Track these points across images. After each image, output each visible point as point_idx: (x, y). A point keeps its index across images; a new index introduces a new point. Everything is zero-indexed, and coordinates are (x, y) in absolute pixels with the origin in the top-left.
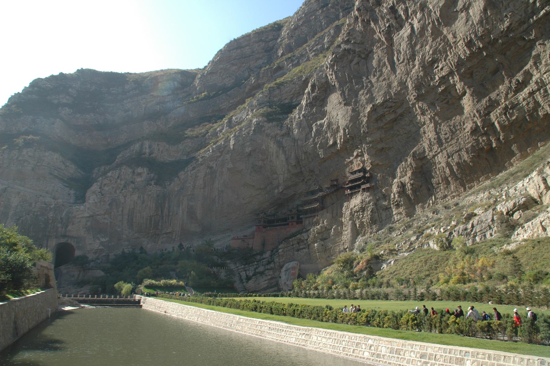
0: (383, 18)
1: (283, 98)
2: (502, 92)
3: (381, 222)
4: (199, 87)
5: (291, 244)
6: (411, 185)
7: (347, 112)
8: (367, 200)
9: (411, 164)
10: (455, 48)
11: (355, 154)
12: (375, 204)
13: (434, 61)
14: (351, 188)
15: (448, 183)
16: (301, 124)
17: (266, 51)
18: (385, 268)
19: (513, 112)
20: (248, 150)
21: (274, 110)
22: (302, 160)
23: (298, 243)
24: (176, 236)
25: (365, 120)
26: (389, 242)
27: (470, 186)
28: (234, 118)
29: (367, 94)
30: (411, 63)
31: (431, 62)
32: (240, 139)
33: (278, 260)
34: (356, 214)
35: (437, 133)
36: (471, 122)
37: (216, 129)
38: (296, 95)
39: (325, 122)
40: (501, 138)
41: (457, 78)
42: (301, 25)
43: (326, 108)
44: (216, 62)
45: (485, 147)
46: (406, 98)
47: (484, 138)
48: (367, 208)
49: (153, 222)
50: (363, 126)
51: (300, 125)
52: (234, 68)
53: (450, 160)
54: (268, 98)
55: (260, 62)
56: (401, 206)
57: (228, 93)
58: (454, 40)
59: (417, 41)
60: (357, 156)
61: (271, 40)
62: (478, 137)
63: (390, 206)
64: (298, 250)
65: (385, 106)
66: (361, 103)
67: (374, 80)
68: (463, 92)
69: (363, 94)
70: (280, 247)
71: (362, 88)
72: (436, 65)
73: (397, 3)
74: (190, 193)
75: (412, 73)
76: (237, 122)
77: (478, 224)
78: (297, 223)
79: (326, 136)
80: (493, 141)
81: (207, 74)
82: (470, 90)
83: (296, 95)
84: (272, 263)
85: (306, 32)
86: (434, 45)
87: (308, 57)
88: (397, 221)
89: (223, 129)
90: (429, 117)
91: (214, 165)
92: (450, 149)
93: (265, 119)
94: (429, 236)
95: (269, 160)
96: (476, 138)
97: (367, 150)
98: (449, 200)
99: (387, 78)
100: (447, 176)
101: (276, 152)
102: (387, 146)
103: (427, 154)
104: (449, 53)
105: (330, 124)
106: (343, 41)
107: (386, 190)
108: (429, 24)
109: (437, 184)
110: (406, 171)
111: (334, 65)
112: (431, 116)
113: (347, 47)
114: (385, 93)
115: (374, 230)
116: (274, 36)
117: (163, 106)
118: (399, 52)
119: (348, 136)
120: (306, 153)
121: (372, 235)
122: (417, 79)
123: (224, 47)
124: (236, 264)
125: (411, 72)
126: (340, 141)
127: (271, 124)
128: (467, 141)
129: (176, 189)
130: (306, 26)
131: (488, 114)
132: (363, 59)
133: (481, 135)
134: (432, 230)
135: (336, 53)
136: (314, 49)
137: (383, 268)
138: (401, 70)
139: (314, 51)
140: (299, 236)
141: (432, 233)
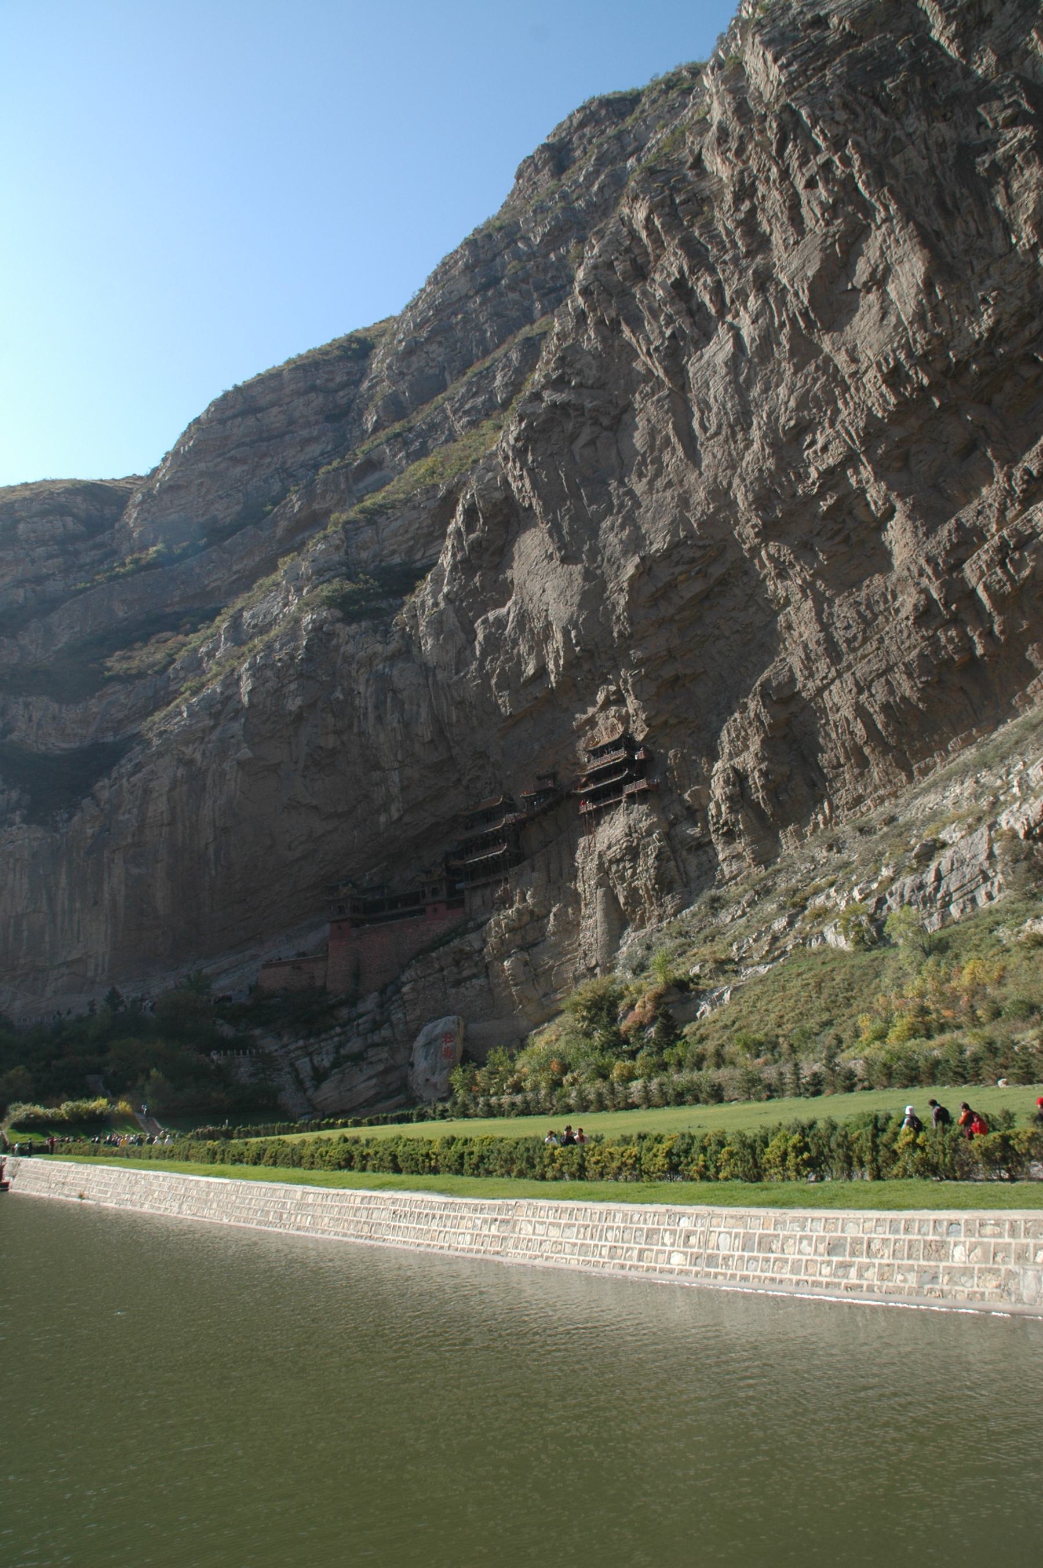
0: (655, 314)
1: (385, 552)
2: (990, 506)
4: (138, 530)
5: (437, 966)
6: (764, 774)
7: (571, 582)
8: (644, 825)
9: (757, 716)
10: (857, 389)
11: (600, 697)
12: (667, 836)
13: (804, 428)
14: (594, 796)
15: (863, 763)
16: (440, 622)
17: (330, 418)
18: (707, 1014)
19: (1022, 558)
20: (294, 704)
21: (361, 586)
23: (457, 963)
24: (96, 969)
25: (623, 600)
26: (712, 940)
27: (923, 766)
28: (246, 615)
29: (622, 527)
30: (740, 436)
31: (794, 431)
33: (400, 1015)
34: (614, 868)
35: (825, 627)
36: (913, 590)
37: (196, 650)
39: (508, 613)
40: (996, 629)
41: (866, 472)
42: (428, 340)
43: (509, 573)
44: (184, 456)
45: (956, 657)
46: (732, 532)
47: (952, 633)
48: (644, 849)
49: (25, 934)
50: (618, 618)
51: (438, 625)
52: (238, 470)
53: (863, 698)
54: (342, 552)
55: (314, 450)
56: (739, 836)
57: (227, 542)
58: (853, 368)
59: (752, 373)
61: (344, 386)
62: (936, 630)
63: (707, 840)
64: (457, 983)
66: (608, 553)
67: (639, 487)
68: (886, 509)
69: (612, 529)
70: (404, 979)
71: (609, 511)
72: (808, 439)
73: (692, 272)
74: (130, 840)
75: (744, 464)
76: (255, 626)
77: (952, 870)
78: (450, 906)
79: (515, 651)
80: (976, 638)
81: (163, 490)
82: (905, 503)
83: (422, 541)
84: (386, 1025)
85: (440, 359)
86: (799, 385)
87: (450, 430)
88: (731, 879)
89: (216, 649)
90: (799, 582)
91: (198, 756)
92: (861, 669)
93: (338, 614)
94: (822, 914)
95: (355, 730)
96: (931, 632)
97: (633, 685)
98: (869, 809)
99: (675, 480)
100: (860, 742)
101: (376, 707)
103: (799, 685)
104: (840, 404)
105: (523, 618)
106: (547, 382)
108: (782, 325)
109: (834, 768)
110: (746, 739)
111: (526, 451)
112: (804, 580)
113: (560, 397)
114: (672, 522)
115: (670, 910)
116: (349, 373)
117: (34, 591)
119: (578, 649)
120: (462, 702)
121: (664, 924)
122: (760, 479)
123: (208, 411)
124: (279, 1036)
125: (742, 459)
126: (557, 665)
127: (354, 626)
128: (907, 644)
129: (90, 832)
130: (440, 343)
131: (958, 566)
132: (606, 429)
133: (942, 626)
134: (828, 897)
135: (529, 416)
136: (467, 407)
137: (703, 1013)
138: (714, 456)
139: (467, 413)
140: (456, 942)
141: (829, 904)
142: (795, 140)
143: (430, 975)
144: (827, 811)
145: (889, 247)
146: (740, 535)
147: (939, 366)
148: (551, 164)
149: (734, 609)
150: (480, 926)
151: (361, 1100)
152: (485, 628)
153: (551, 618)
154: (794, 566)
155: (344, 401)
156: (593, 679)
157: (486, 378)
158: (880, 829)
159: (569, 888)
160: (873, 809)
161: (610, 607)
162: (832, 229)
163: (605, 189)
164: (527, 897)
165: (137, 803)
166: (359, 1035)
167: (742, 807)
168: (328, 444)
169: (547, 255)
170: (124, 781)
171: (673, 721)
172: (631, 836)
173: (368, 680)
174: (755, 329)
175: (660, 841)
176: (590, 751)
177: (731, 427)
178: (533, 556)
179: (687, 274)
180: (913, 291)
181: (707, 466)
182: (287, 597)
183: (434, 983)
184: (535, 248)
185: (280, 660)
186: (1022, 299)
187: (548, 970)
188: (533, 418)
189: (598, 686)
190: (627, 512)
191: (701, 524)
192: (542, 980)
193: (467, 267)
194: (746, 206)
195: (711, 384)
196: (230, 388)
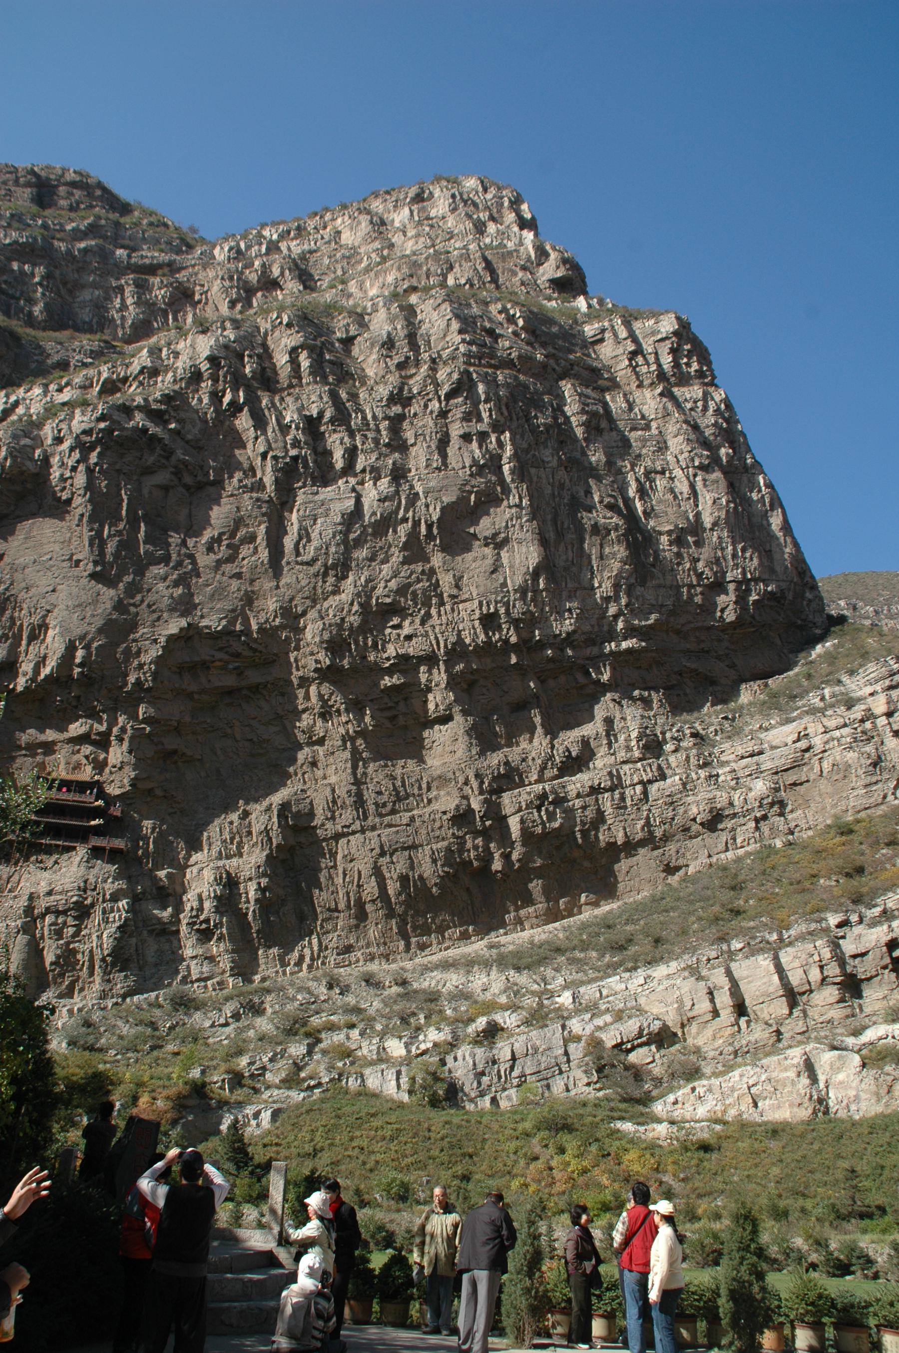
0: (284, 429)
3: (140, 969)
7: (95, 601)
8: (110, 887)
9: (267, 831)
10: (453, 610)
12: (131, 909)
13: (393, 610)
15: (361, 915)
19: (554, 813)
25: (155, 652)
29: (176, 584)
30: (331, 580)
31: (385, 607)
34: (49, 919)
35: (357, 783)
36: (455, 793)
40: (515, 856)
41: (440, 676)
47: (479, 841)
50: (141, 666)
53: (383, 861)
56: (219, 939)
58: (455, 592)
60: (83, 739)
62: (466, 834)
67: (204, 560)
71: (166, 559)
73: (332, 421)
75: (326, 605)
80: (497, 856)
88: (198, 980)
96: (460, 833)
97: (132, 738)
98: (358, 961)
100: (366, 896)
102: (189, 752)
103: (317, 822)
104: (433, 611)
107: (169, 876)
108: (405, 520)
109: (329, 910)
111: (92, 448)
112: (347, 732)
113: (153, 429)
114: (233, 611)
115: (119, 988)
118: (304, 535)
121: (110, 1003)
122: (340, 626)
125: (325, 599)
126: (37, 670)
128: (437, 833)
131: (499, 791)
132: (187, 487)
133: (472, 833)
135: (113, 422)
142: (466, 398)
144: (316, 948)
145: (513, 526)
146: (296, 660)
147: (525, 635)
148: (35, 190)
153: (51, 621)
154: (340, 715)
156: (76, 707)
158: (390, 987)
160: (361, 963)
161: (134, 650)
162: (473, 482)
163: (89, 254)
171: (159, 792)
172: (85, 891)
174: (379, 507)
175: (127, 912)
177: (327, 568)
178: (48, 548)
179: (325, 420)
180: (524, 570)
181: (288, 585)
186: (592, 626)
189: (81, 717)
190: (185, 573)
191: (261, 630)
194: (397, 409)
195: (319, 521)
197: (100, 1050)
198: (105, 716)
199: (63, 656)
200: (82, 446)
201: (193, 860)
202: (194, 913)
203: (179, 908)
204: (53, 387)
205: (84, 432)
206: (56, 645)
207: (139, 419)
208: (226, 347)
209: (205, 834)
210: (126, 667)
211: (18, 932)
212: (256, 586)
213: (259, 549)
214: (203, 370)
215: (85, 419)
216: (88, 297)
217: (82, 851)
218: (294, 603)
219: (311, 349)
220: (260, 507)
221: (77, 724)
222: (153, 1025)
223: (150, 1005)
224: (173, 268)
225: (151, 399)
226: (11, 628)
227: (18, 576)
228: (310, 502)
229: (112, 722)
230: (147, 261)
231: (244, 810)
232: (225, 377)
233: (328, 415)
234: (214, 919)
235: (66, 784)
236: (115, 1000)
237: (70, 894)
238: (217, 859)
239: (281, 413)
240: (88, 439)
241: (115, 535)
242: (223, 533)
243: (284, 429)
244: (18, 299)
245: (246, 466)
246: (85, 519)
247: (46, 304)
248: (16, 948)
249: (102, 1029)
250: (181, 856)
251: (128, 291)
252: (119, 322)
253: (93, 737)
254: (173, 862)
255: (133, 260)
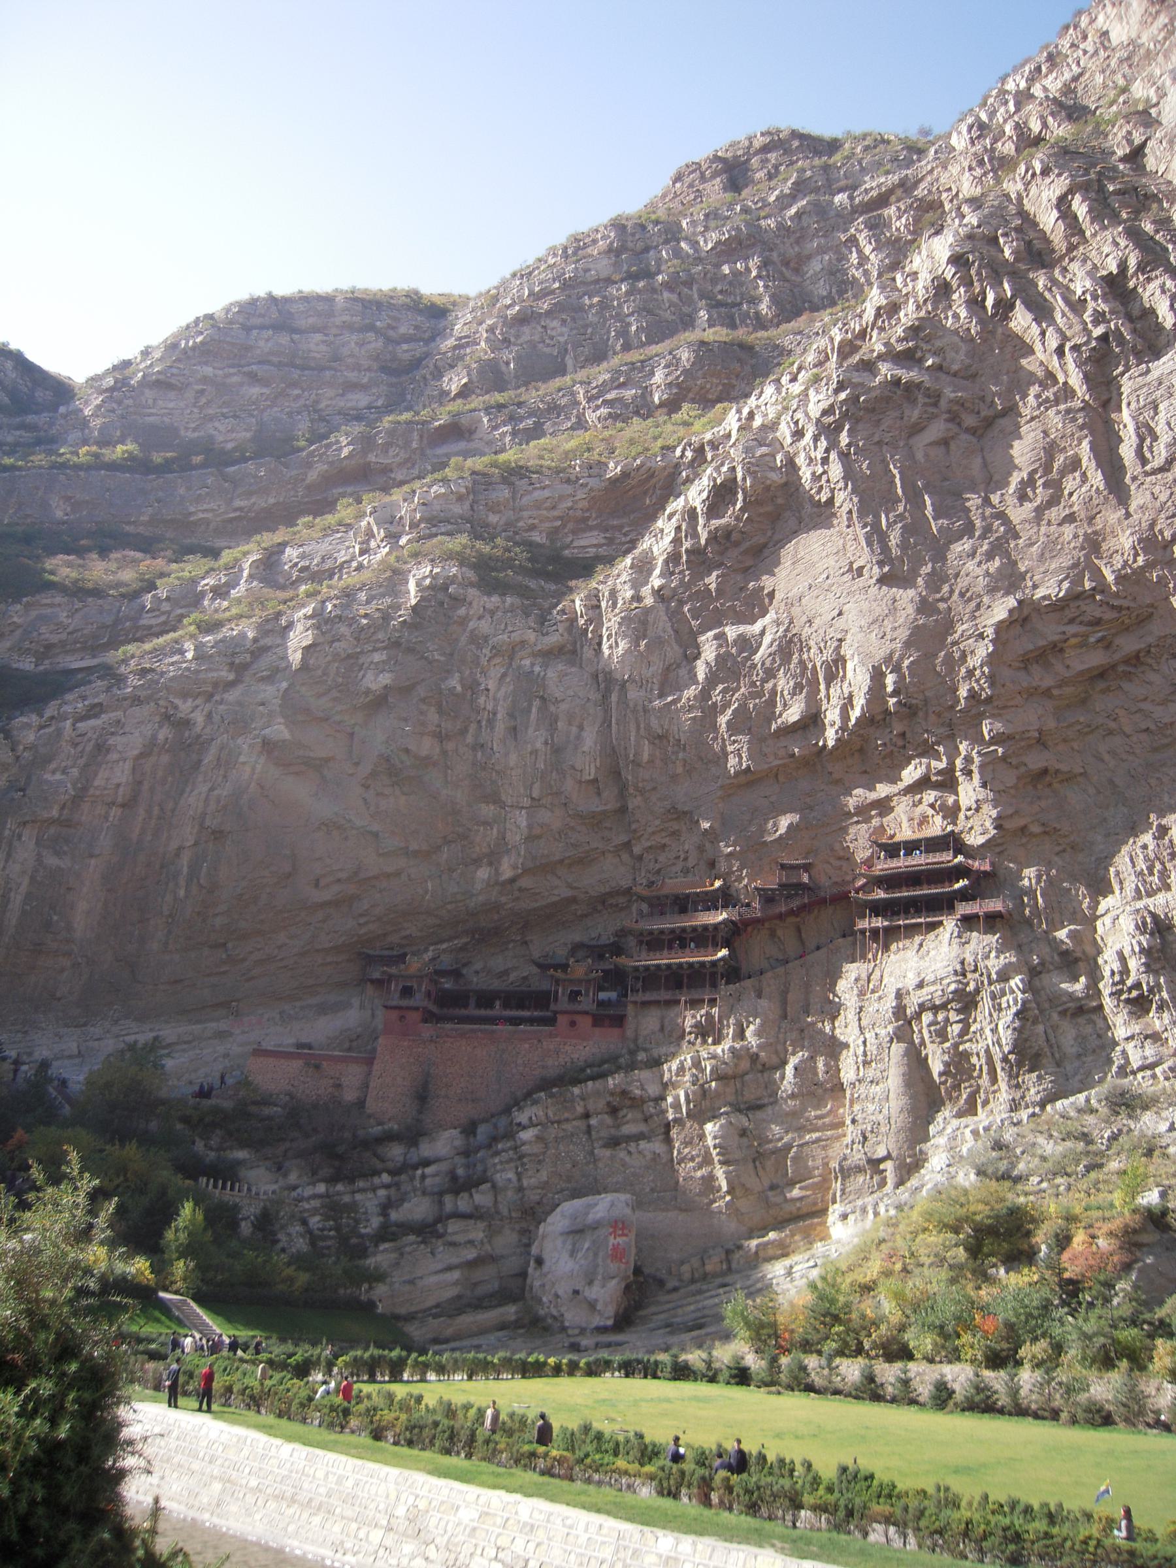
0: (1077, 306)
1: (521, 524)
3: (1058, 1065)
5: (580, 1109)
7: (893, 610)
8: (995, 964)
12: (1029, 987)
14: (878, 909)
20: (376, 681)
21: (498, 552)
22: (637, 764)
23: (613, 1111)
25: (983, 650)
28: (291, 553)
32: (343, 629)
33: (511, 1175)
34: (927, 1018)
37: (194, 581)
38: (570, 526)
39: (763, 633)
42: (549, 313)
43: (767, 582)
44: (185, 351)
46: (1167, 598)
50: (970, 673)
52: (255, 391)
55: (360, 400)
56: (1160, 1008)
57: (232, 469)
60: (923, 784)
64: (614, 1142)
65: (1070, 613)
66: (962, 583)
67: (1018, 514)
69: (972, 554)
71: (969, 529)
73: (1141, 268)
76: (302, 570)
78: (598, 1021)
81: (143, 383)
83: (570, 526)
84: (483, 1187)
85: (562, 339)
87: (578, 417)
88: (1142, 1068)
91: (199, 718)
93: (471, 575)
95: (469, 739)
97: (982, 767)
99: (1083, 516)
101: (511, 715)
102: (1064, 767)
105: (788, 647)
107: (1071, 935)
111: (839, 428)
113: (906, 375)
114: (1075, 566)
116: (416, 327)
118: (1146, 433)
120: (660, 737)
121: (1024, 1115)
126: (845, 716)
127: (495, 599)
130: (564, 321)
132: (972, 431)
135: (855, 386)
136: (609, 397)
139: (606, 403)
143: (567, 1120)
149: (1145, 699)
150: (657, 1063)
151: (430, 1303)
152: (720, 646)
153: (846, 651)
155: (407, 356)
156: (904, 747)
157: (642, 370)
159: (821, 1032)
161: (957, 655)
164: (749, 1032)
165: (81, 762)
166: (424, 1193)
167: (1163, 968)
168: (379, 397)
169: (718, 266)
170: (69, 723)
171: (1036, 829)
172: (964, 975)
173: (504, 675)
175: (1023, 992)
176: (883, 847)
178: (820, 566)
179: (1131, 271)
182: (367, 542)
183: (572, 1135)
184: (703, 254)
185: (366, 616)
187: (780, 1150)
188: (860, 390)
189: (912, 758)
190: (997, 539)
191: (1120, 579)
192: (770, 1163)
193: (610, 250)
195: (1161, 407)
196: (262, 294)
197: (1018, 1179)
198: (941, 749)
199: (870, 689)
200: (828, 431)
201: (1101, 909)
202: (1117, 978)
203: (1095, 976)
204: (785, 380)
205: (825, 413)
206: (859, 678)
207: (886, 370)
208: (970, 237)
209: (1112, 870)
210: (952, 680)
211: (891, 1041)
212: (1099, 523)
213: (1089, 474)
214: (948, 278)
215: (821, 397)
216: (818, 267)
217: (950, 924)
218: (1157, 529)
219: (1083, 188)
220: (1074, 420)
221: (911, 767)
222: (1086, 1138)
223: (1079, 1111)
224: (906, 186)
225: (893, 341)
226: (803, 674)
227: (795, 611)
228: (1140, 388)
229: (953, 753)
230: (874, 193)
231: (1160, 826)
232: (979, 274)
233: (1132, 262)
234: (1146, 981)
235: (911, 847)
236: (1030, 1110)
237: (945, 982)
238: (1134, 899)
239: (1068, 288)
240: (831, 419)
241: (895, 522)
242: (1035, 471)
243: (1077, 306)
244: (741, 304)
245: (1040, 374)
246: (855, 515)
247: (772, 297)
248: (893, 1061)
249: (1018, 1151)
250: (1085, 906)
251: (862, 238)
252: (863, 280)
253: (934, 778)
254: (1075, 916)
255: (857, 201)
